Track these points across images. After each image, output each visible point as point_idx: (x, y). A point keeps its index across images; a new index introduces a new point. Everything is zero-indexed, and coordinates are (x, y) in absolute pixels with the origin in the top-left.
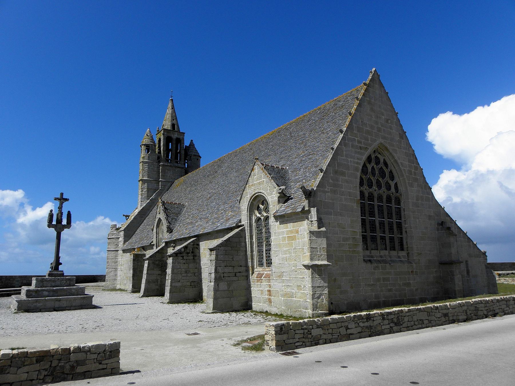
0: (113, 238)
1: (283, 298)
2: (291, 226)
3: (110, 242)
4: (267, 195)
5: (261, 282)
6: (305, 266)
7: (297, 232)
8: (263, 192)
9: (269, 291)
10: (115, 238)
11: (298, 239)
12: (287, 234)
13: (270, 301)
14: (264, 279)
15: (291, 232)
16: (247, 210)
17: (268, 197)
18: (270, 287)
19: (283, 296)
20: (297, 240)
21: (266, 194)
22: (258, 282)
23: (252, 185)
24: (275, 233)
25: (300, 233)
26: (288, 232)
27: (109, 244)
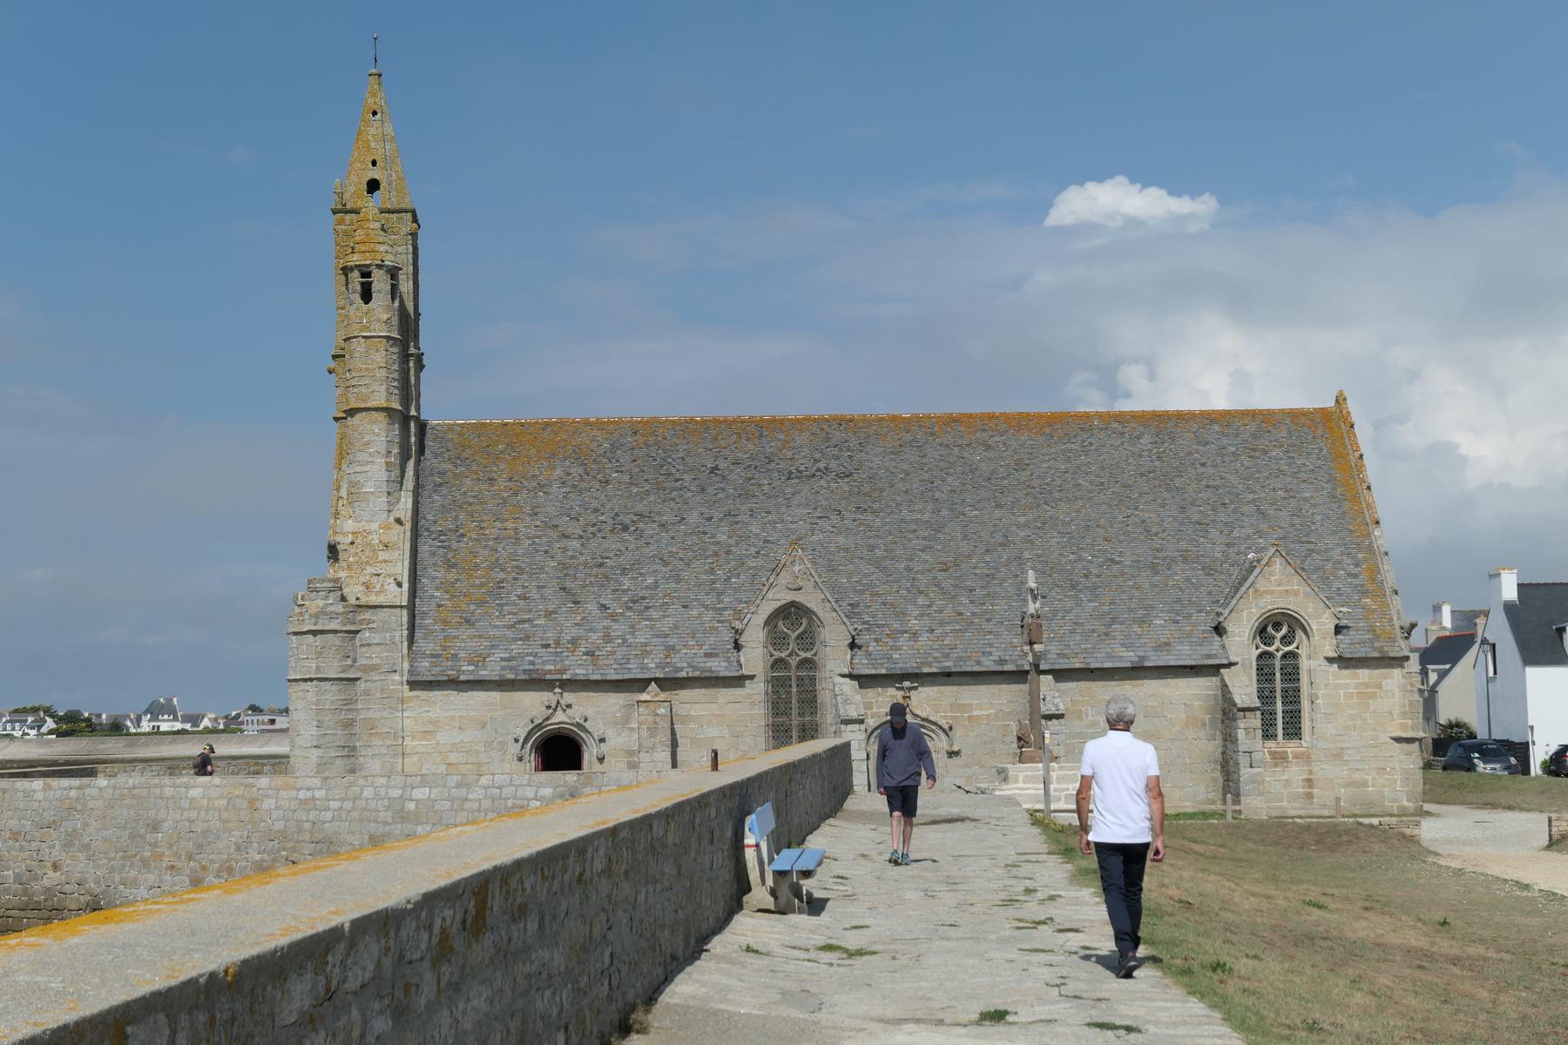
0: (335, 632)
1: (1343, 790)
2: (1364, 674)
3: (324, 647)
4: (1306, 617)
5: (1287, 767)
6: (1398, 740)
7: (1379, 686)
8: (1296, 609)
9: (1309, 781)
10: (341, 631)
11: (1381, 697)
12: (1355, 689)
13: (1310, 796)
14: (1294, 761)
15: (1367, 685)
16: (1249, 637)
17: (1310, 622)
18: (1310, 774)
19: (1348, 785)
20: (1379, 700)
21: (1303, 614)
22: (1276, 765)
23: (1265, 592)
24: (1326, 685)
25: (1384, 689)
26: (1358, 686)
27: (321, 653)
